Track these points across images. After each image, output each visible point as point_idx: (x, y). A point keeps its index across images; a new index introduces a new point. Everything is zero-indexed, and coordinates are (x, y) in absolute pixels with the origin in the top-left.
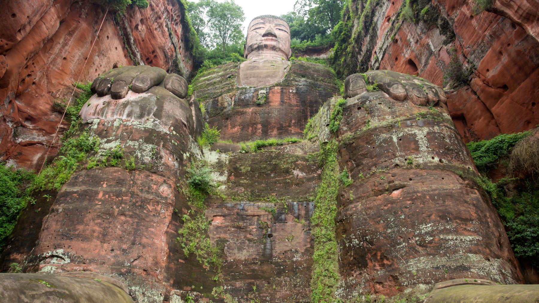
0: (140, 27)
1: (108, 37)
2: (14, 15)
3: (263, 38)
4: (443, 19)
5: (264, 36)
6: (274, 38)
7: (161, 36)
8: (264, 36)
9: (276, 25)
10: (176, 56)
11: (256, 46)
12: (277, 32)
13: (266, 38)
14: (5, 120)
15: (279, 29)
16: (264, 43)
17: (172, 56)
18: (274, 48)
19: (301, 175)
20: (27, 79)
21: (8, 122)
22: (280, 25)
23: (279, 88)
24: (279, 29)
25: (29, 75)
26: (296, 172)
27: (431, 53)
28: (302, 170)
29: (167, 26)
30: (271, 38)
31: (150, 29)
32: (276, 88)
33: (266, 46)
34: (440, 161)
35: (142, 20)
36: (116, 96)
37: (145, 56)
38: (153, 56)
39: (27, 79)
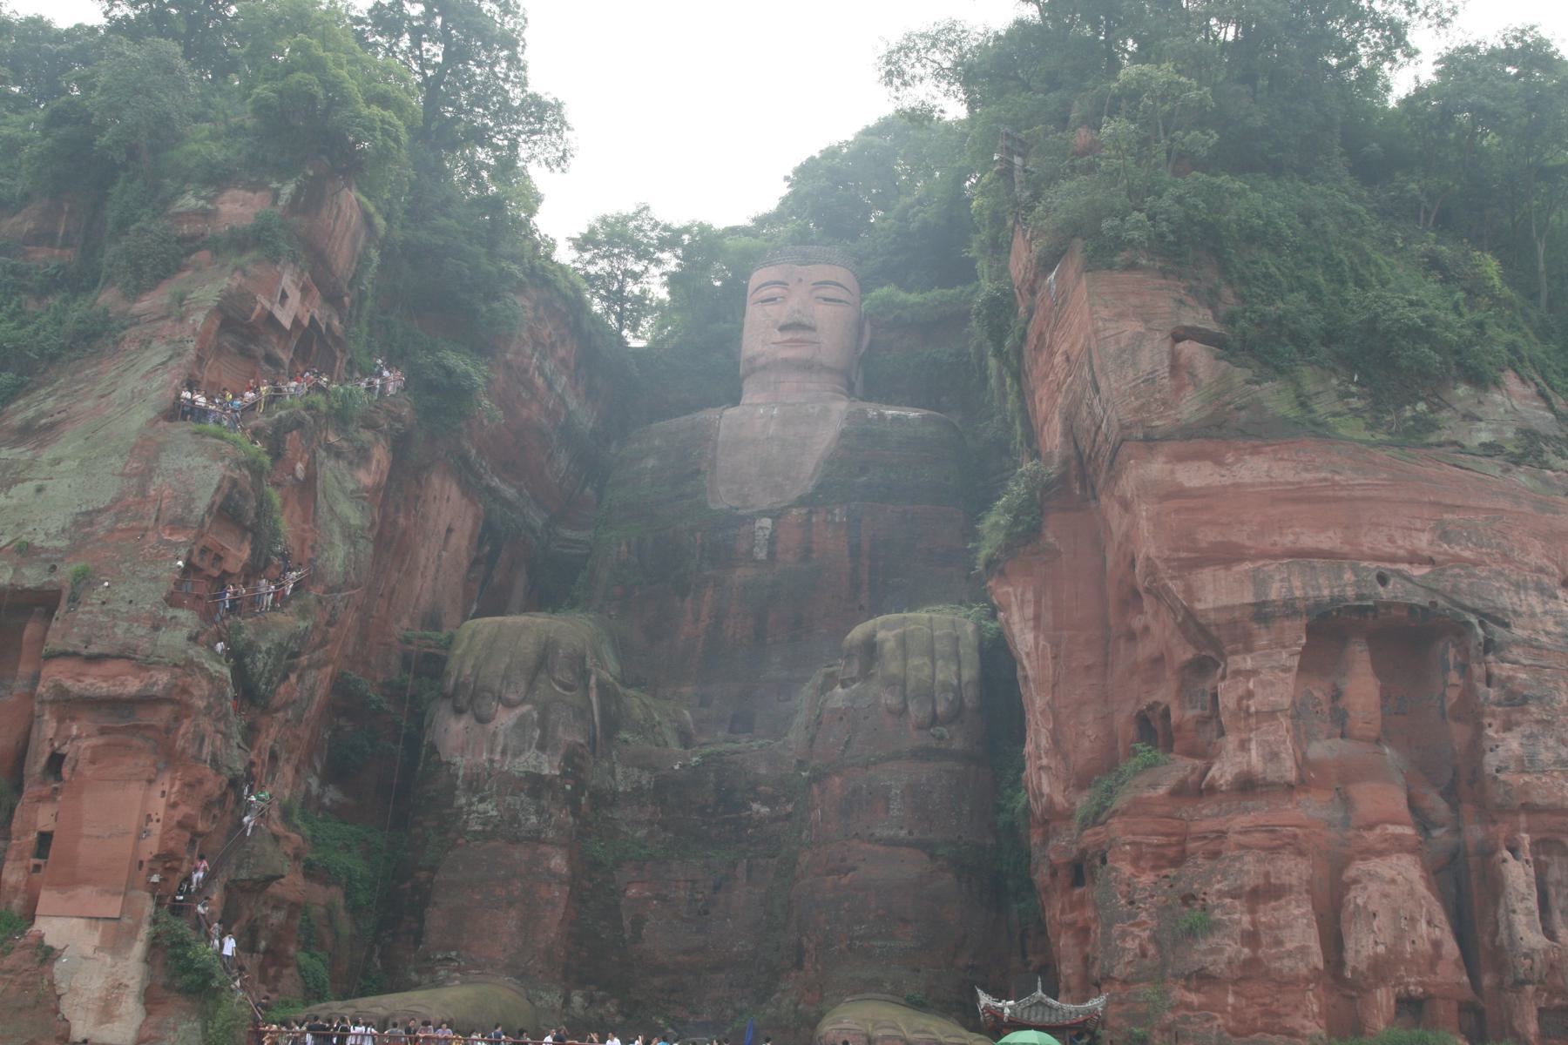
5: (783, 329)
11: (762, 360)
13: (788, 336)
19: (765, 810)
23: (804, 511)
26: (755, 806)
28: (764, 804)
32: (794, 512)
34: (910, 833)
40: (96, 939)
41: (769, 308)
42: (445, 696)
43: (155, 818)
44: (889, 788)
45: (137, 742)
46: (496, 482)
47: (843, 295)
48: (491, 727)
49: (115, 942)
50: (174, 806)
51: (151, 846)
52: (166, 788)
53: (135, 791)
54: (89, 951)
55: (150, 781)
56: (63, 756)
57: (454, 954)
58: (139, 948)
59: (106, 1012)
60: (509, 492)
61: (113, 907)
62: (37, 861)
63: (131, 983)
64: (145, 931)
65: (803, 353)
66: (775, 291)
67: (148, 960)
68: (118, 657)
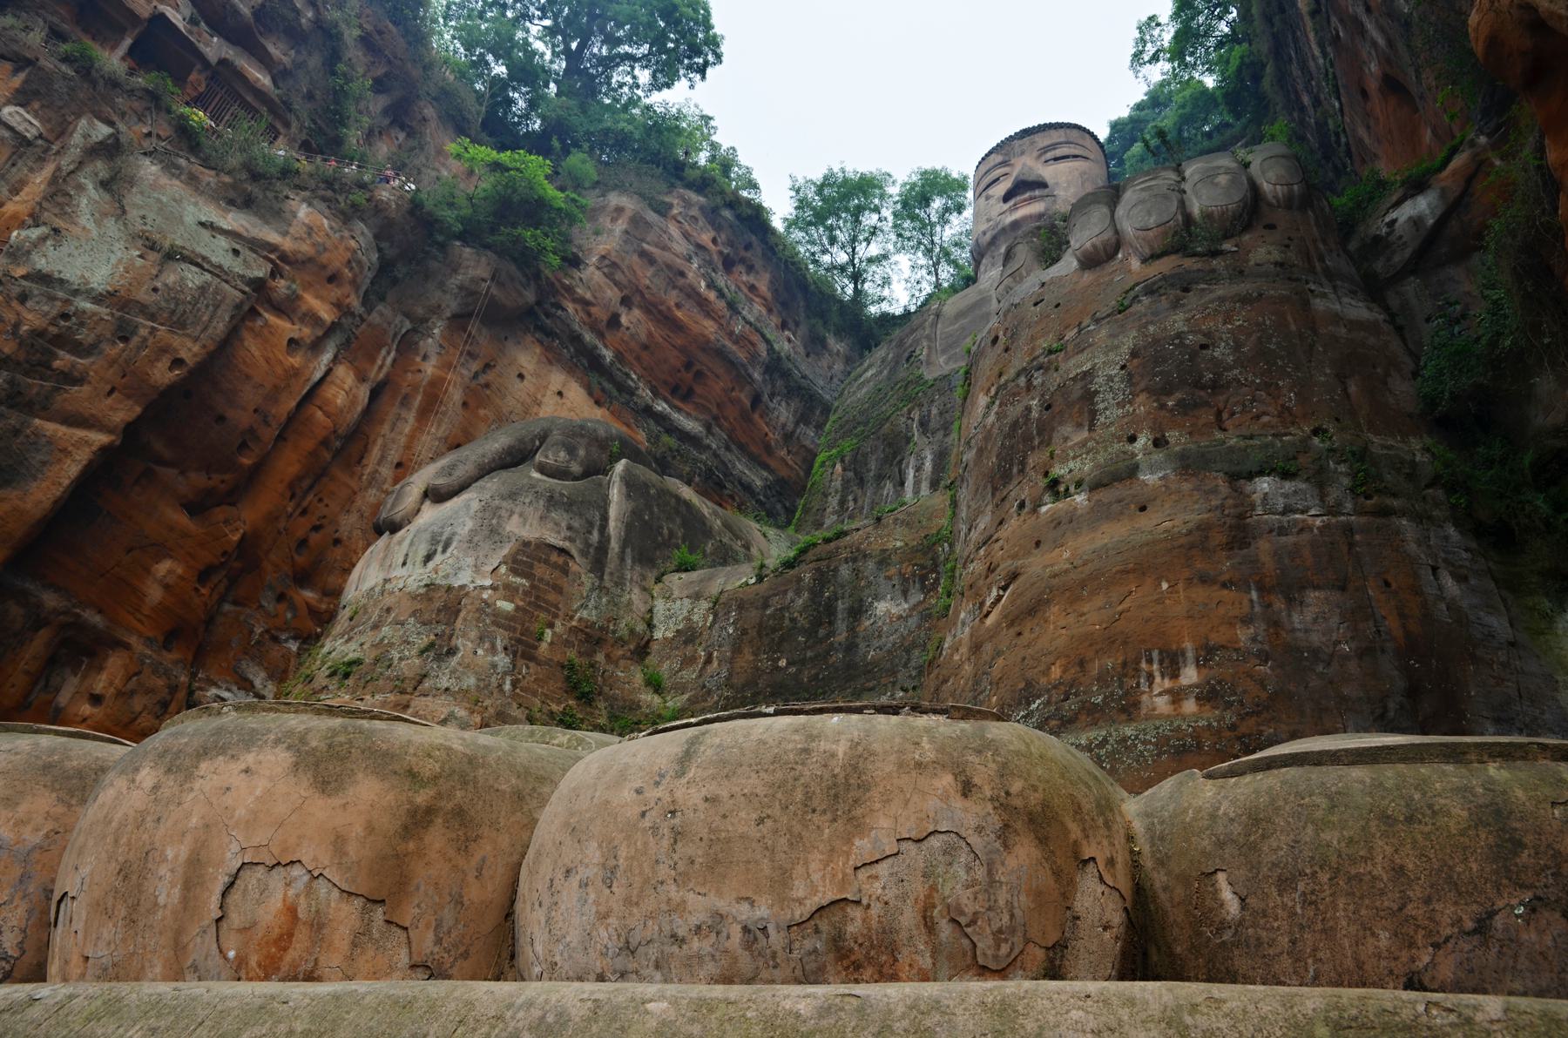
0: (624, 320)
1: (521, 376)
2: (221, 419)
7: (700, 317)
8: (1006, 199)
9: (1045, 150)
10: (771, 349)
11: (988, 236)
12: (1047, 172)
13: (1011, 203)
14: (275, 639)
15: (1056, 159)
16: (1009, 219)
17: (754, 357)
20: (315, 537)
21: (286, 641)
22: (1053, 146)
24: (1056, 159)
25: (316, 528)
29: (711, 285)
31: (660, 312)
35: (626, 302)
37: (665, 382)
38: (690, 376)
39: (315, 537)
41: (991, 192)
46: (661, 406)
47: (1077, 152)
60: (691, 425)
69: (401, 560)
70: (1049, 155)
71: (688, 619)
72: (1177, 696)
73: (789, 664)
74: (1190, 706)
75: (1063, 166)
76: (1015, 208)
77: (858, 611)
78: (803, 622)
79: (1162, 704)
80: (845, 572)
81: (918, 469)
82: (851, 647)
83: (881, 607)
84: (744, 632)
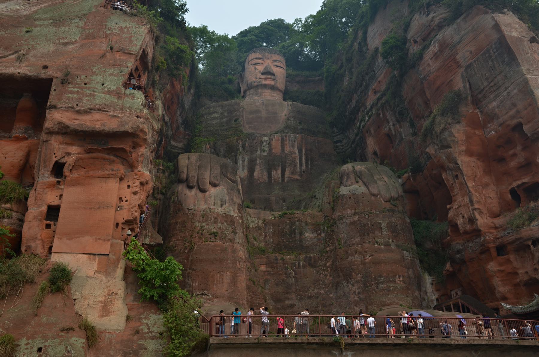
3: (263, 77)
4: (411, 119)
5: (263, 74)
6: (272, 77)
11: (256, 84)
16: (264, 82)
18: (273, 88)
27: (402, 139)
30: (270, 77)
33: (265, 86)
36: (203, 191)
40: (95, 266)
42: (180, 181)
43: (124, 200)
44: (380, 224)
45: (112, 157)
47: (282, 66)
48: (207, 193)
49: (106, 269)
50: (135, 193)
51: (124, 216)
52: (130, 183)
53: (113, 185)
54: (91, 273)
55: (121, 179)
56: (64, 164)
57: (206, 292)
58: (120, 272)
59: (106, 309)
61: (105, 248)
62: (48, 222)
63: (119, 292)
64: (122, 264)
65: (272, 83)
66: (260, 61)
67: (125, 278)
68: (99, 110)
69: (213, 204)
70: (275, 63)
71: (258, 224)
72: (400, 281)
73: (287, 241)
74: (402, 283)
75: (279, 69)
76: (265, 79)
77: (301, 234)
78: (288, 232)
79: (399, 282)
80: (297, 223)
81: (243, 161)
82: (301, 241)
83: (307, 234)
84: (275, 231)
